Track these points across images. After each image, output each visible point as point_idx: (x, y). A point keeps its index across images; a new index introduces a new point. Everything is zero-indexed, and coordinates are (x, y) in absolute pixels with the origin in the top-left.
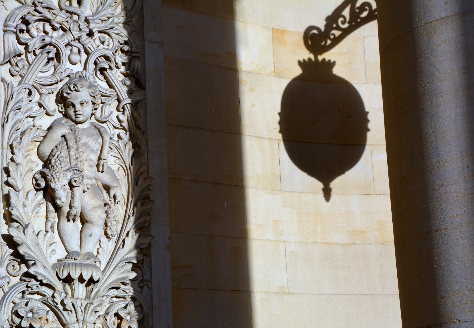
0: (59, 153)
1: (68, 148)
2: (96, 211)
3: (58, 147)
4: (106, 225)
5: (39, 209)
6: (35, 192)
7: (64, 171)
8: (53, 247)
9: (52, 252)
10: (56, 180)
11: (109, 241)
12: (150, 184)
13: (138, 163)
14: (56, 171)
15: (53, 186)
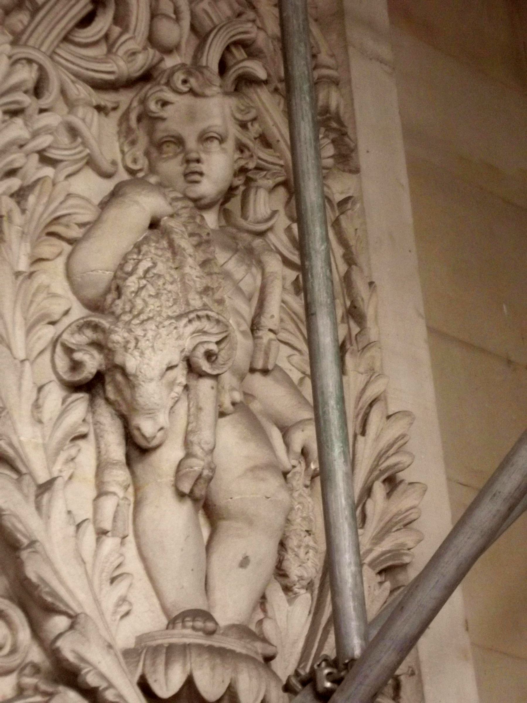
0: (146, 264)
1: (174, 253)
2: (263, 480)
3: (144, 248)
4: (282, 545)
5: (73, 452)
6: (64, 393)
7: (169, 317)
8: (121, 588)
9: (118, 605)
10: (143, 344)
11: (290, 601)
12: (403, 436)
13: (361, 370)
14: (143, 317)
15: (131, 363)
